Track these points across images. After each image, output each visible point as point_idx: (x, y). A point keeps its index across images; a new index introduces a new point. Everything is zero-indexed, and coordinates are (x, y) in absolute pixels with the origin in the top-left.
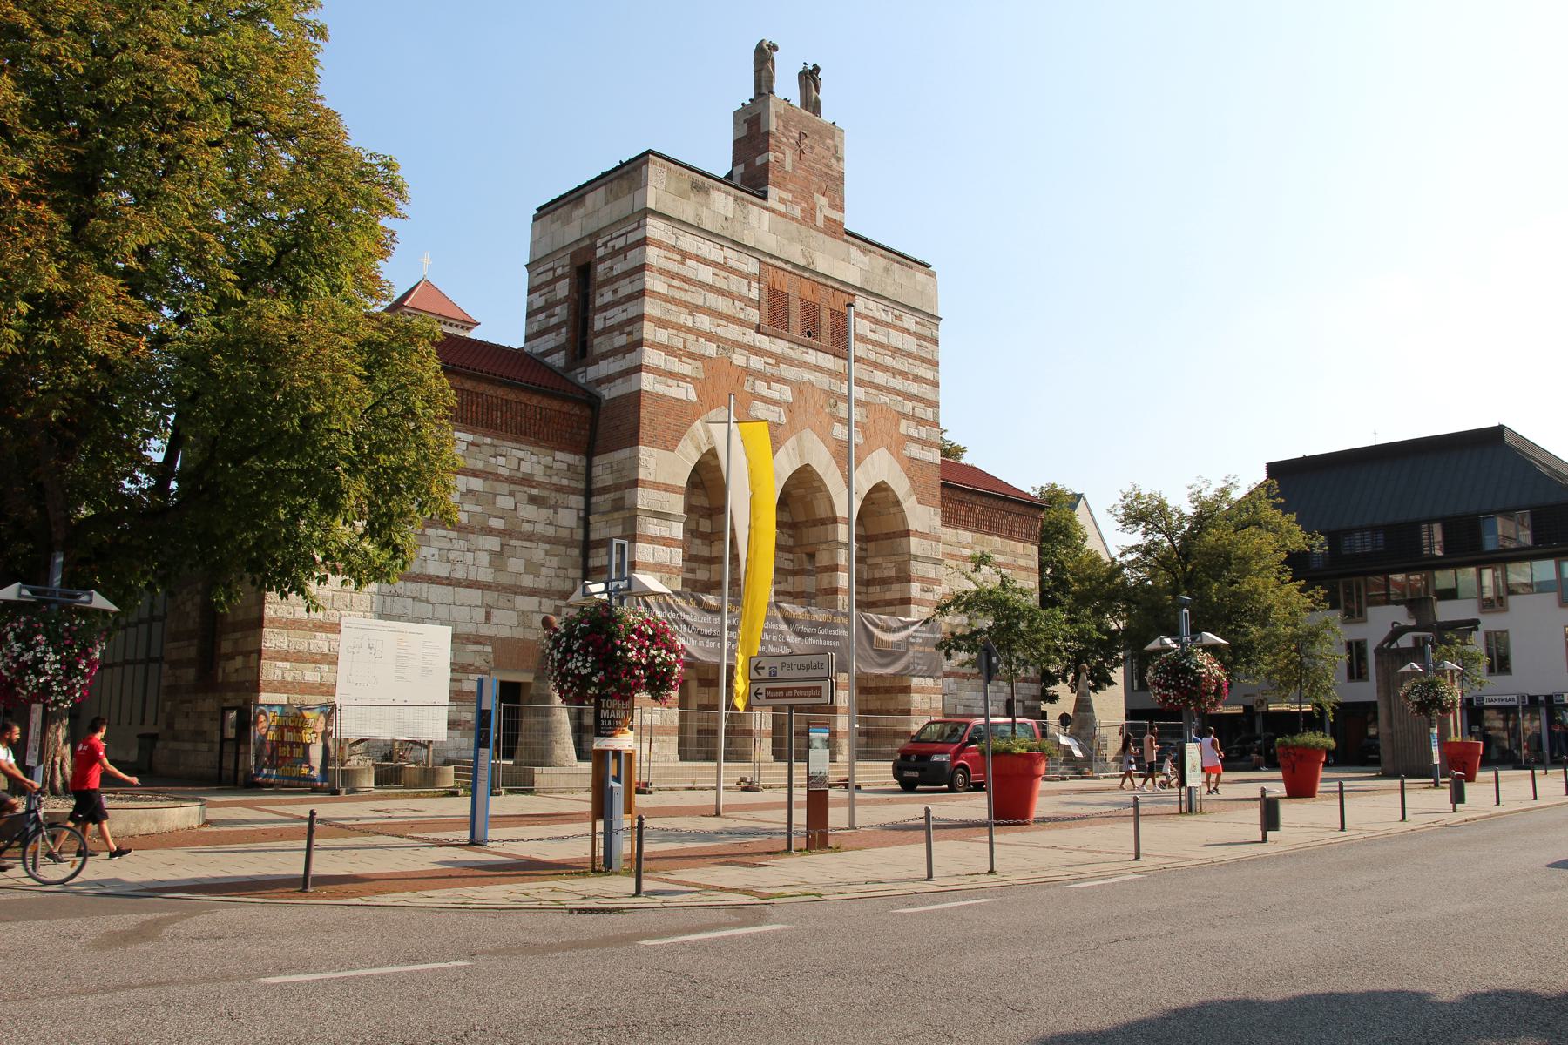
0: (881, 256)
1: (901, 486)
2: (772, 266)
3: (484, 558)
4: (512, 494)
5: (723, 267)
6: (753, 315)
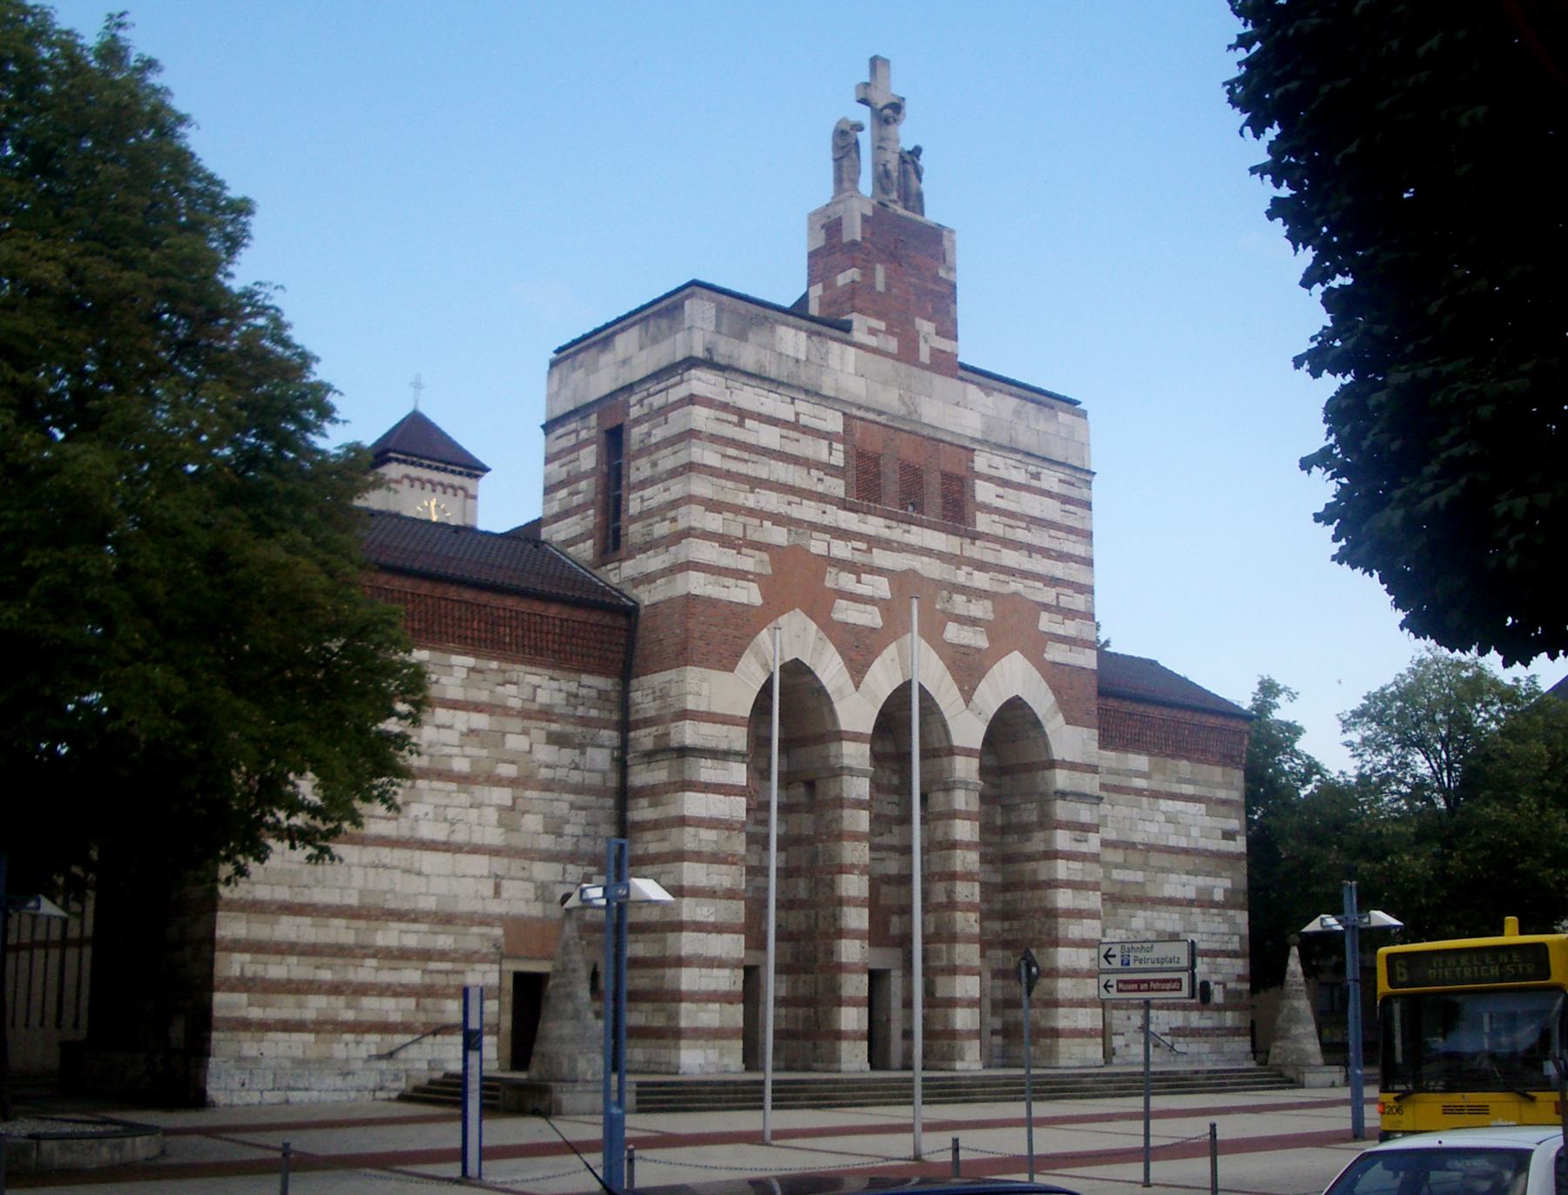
0: (1011, 394)
1: (1041, 701)
2: (862, 419)
3: (491, 815)
4: (525, 732)
5: (795, 426)
6: (837, 487)
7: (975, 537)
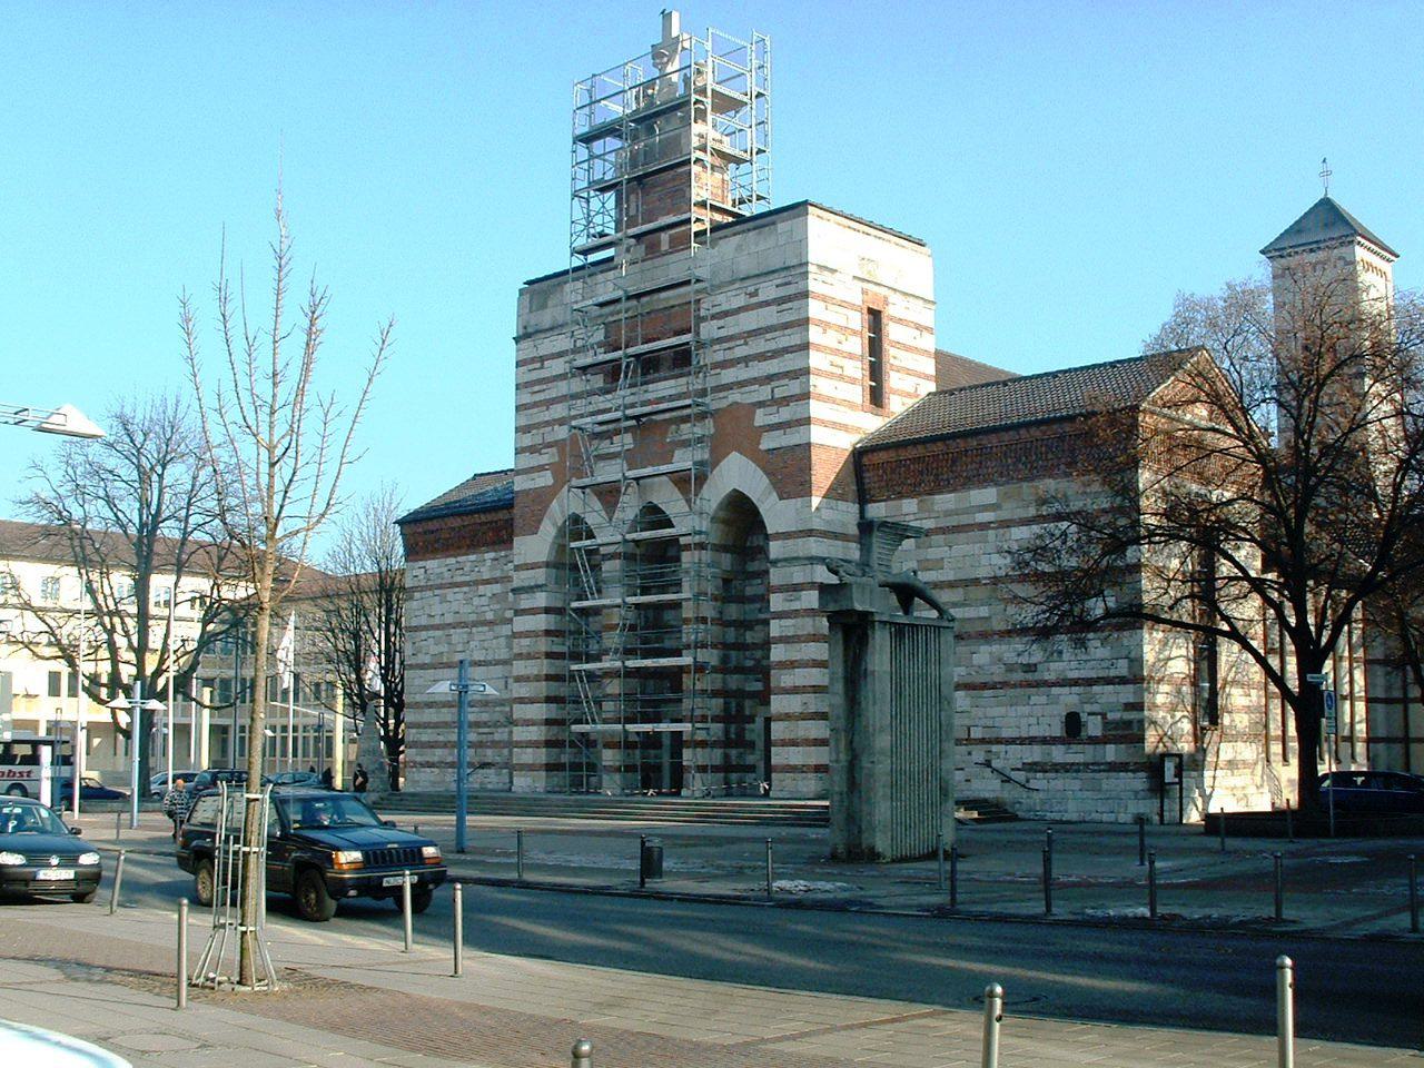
0: (735, 235)
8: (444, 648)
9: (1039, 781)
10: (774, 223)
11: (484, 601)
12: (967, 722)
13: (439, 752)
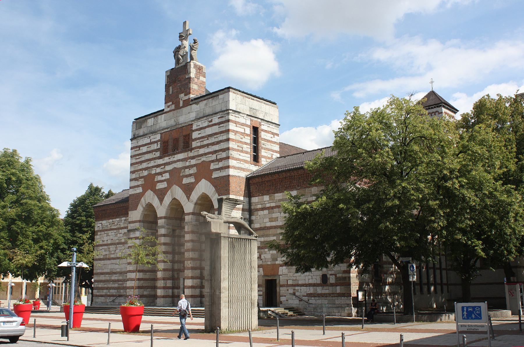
6: (158, 154)
7: (191, 150)
8: (108, 253)
9: (312, 301)
10: (218, 95)
11: (121, 235)
12: (286, 278)
13: (105, 291)
